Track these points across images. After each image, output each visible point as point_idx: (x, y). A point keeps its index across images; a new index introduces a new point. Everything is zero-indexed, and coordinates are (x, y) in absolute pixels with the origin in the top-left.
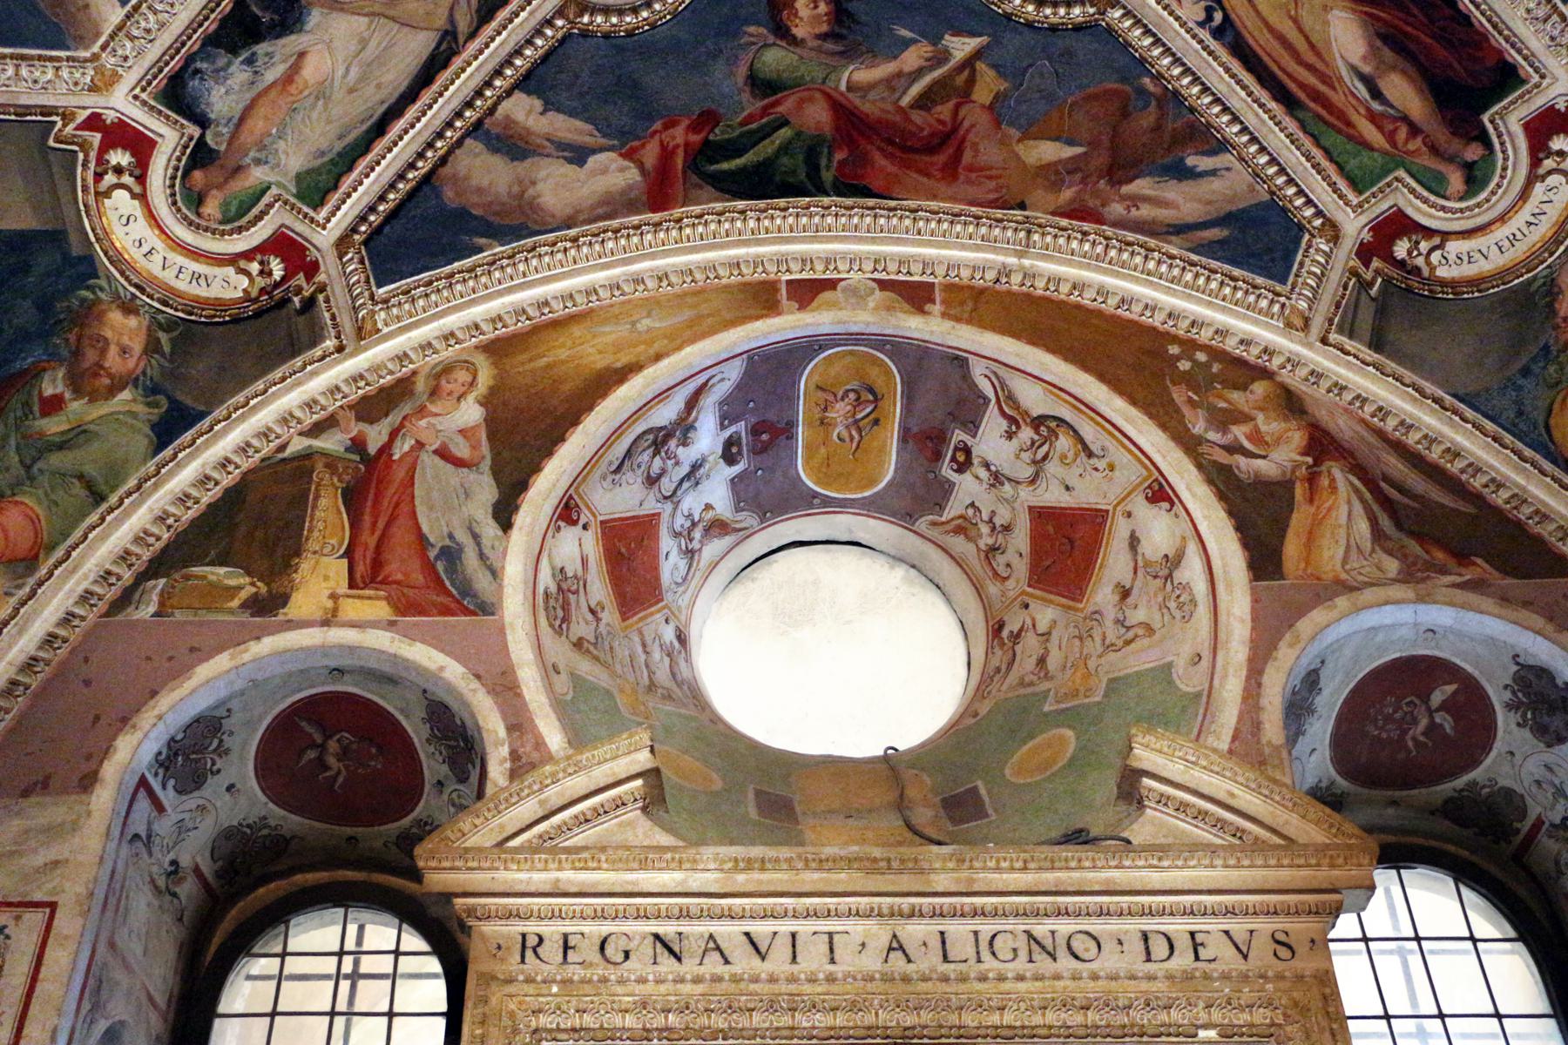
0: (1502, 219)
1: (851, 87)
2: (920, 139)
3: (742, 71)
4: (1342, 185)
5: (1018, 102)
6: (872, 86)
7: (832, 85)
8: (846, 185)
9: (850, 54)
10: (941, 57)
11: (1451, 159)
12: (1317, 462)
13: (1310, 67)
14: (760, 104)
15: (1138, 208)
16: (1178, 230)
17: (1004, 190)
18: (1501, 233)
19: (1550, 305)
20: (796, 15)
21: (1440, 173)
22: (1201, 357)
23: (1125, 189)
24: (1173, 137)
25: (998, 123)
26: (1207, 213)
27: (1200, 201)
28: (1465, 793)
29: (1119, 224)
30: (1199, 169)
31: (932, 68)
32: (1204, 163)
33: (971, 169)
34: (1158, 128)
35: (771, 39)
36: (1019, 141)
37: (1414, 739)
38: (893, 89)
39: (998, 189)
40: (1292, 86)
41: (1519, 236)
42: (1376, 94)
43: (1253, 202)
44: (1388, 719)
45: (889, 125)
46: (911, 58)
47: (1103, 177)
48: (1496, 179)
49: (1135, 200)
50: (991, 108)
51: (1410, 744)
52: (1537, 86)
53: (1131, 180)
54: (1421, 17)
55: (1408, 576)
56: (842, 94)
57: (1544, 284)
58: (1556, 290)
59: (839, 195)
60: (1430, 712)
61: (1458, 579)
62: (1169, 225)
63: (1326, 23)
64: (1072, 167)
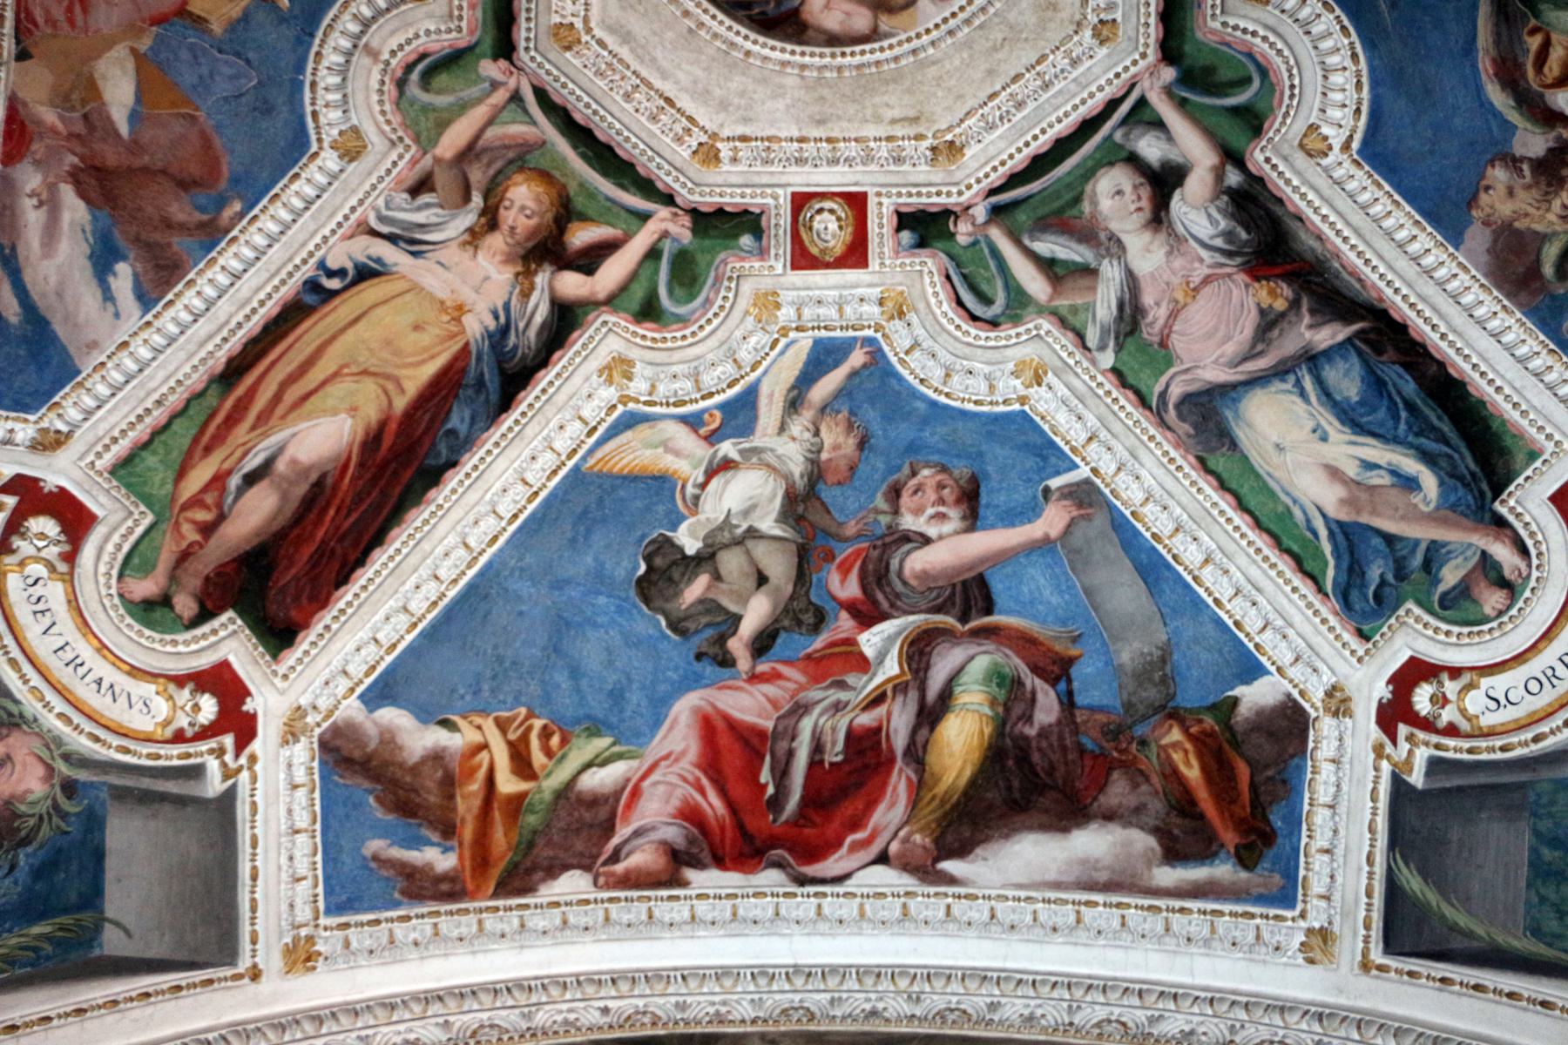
0: (102, 649)
5: (192, 48)
11: (173, 577)
13: (277, 398)
17: (49, 31)
18: (85, 651)
21: (154, 567)
23: (68, 193)
24: (158, 244)
25: (158, 21)
26: (44, 295)
27: (61, 283)
30: (111, 279)
32: (123, 277)
34: (169, 224)
36: (134, 51)
40: (249, 380)
41: (81, 671)
42: (251, 479)
43: (72, 350)
47: (82, 159)
48: (157, 636)
49: (51, 203)
52: (275, 673)
53: (82, 195)
54: (346, 525)
57: (10, 714)
63: (335, 412)
64: (94, 121)
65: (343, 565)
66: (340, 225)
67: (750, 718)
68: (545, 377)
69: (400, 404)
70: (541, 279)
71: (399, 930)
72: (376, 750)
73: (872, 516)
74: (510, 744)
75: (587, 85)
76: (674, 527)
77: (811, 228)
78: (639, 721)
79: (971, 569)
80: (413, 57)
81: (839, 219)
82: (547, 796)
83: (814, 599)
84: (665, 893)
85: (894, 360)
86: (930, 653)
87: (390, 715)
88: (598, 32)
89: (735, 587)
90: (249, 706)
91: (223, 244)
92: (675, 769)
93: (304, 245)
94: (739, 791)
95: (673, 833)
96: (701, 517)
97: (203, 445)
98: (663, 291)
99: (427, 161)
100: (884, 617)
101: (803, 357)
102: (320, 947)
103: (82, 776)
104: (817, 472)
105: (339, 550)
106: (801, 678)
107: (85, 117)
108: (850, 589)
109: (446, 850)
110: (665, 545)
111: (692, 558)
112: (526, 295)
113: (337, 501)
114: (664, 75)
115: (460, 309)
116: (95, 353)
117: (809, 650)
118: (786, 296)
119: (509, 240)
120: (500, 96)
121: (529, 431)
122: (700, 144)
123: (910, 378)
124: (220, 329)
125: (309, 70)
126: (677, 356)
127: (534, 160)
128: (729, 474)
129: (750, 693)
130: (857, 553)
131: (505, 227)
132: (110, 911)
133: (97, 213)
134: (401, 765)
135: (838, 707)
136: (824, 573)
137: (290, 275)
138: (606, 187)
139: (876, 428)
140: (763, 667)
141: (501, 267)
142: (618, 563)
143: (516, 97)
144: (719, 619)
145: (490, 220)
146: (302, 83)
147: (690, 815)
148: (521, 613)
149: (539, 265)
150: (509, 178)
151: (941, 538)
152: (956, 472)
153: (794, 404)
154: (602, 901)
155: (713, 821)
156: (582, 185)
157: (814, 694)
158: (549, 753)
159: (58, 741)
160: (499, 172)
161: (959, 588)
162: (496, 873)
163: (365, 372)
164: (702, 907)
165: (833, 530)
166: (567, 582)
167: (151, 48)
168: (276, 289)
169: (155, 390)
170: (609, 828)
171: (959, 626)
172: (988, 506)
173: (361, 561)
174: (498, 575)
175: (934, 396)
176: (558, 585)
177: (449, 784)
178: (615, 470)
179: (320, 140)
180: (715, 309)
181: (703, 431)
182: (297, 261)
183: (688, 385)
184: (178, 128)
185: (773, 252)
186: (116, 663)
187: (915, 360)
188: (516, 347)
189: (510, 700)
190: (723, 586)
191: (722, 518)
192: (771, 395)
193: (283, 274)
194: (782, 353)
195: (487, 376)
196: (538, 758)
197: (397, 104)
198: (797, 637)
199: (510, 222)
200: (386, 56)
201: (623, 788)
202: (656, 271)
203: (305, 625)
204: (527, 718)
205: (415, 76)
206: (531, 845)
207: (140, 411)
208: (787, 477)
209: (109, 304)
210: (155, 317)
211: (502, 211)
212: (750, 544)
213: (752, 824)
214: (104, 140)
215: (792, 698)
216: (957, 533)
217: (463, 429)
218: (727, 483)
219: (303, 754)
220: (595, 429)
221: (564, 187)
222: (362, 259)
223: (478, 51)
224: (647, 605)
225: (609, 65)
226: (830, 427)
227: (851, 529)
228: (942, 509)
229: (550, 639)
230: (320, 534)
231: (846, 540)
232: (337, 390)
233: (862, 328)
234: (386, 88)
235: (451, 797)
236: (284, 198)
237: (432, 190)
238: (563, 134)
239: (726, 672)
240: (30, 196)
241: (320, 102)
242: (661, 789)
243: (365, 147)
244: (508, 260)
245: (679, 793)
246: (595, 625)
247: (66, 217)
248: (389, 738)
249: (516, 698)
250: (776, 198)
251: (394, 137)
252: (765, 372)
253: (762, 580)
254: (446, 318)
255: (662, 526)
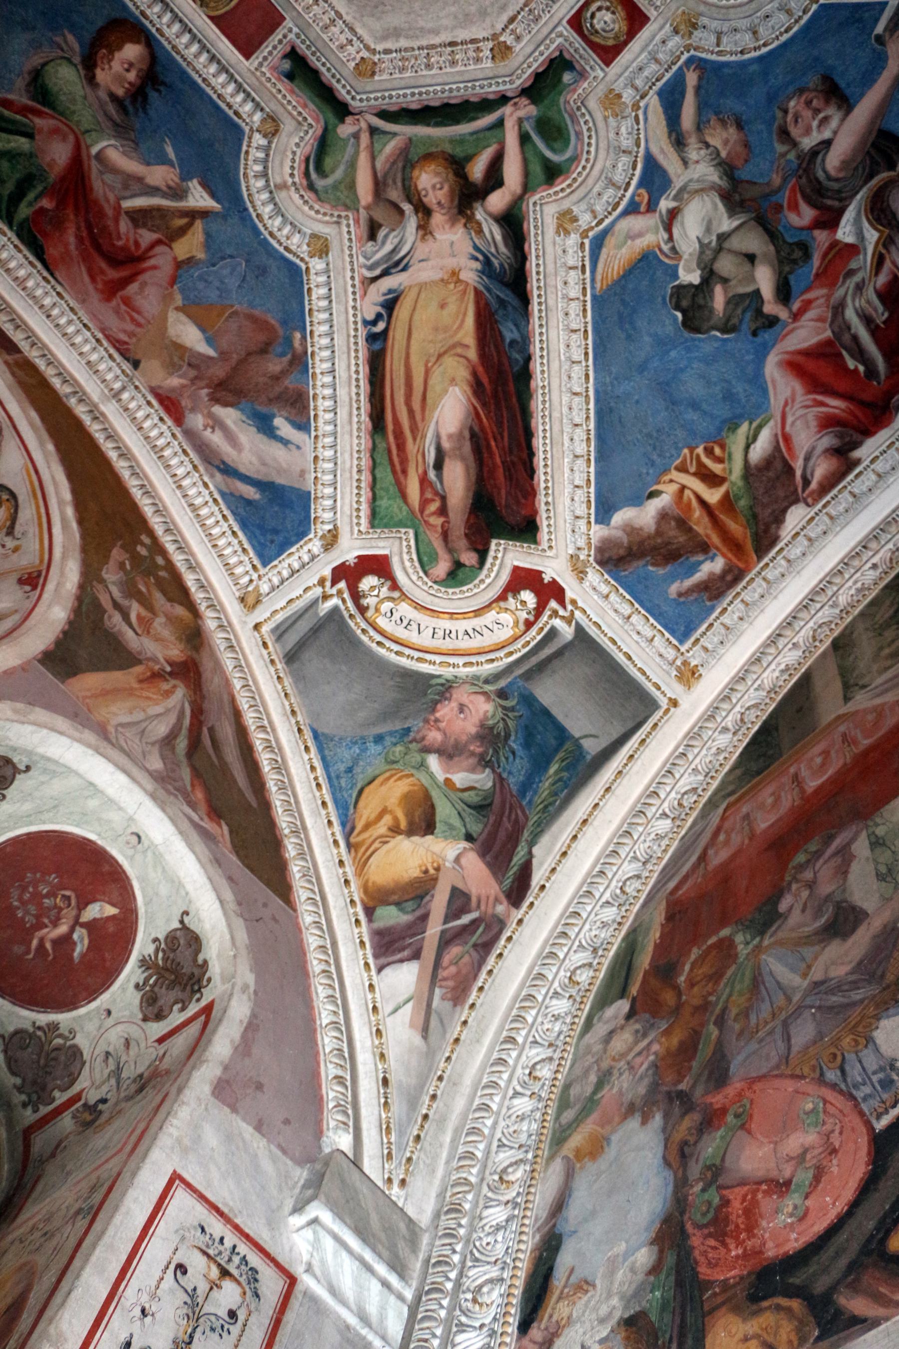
1: (99, 157)
2: (114, 245)
3: (36, 60)
4: (365, 508)
5: (201, 278)
6: (115, 170)
7: (89, 141)
8: (30, 231)
9: (121, 130)
10: (178, 193)
11: (450, 550)
12: (171, 674)
13: (411, 412)
14: (25, 101)
15: (213, 431)
16: (228, 470)
17: (134, 340)
18: (446, 624)
19: (436, 703)
20: (110, 61)
21: (437, 554)
22: (160, 561)
24: (281, 393)
25: (173, 281)
26: (258, 472)
28: (39, 1033)
29: (190, 435)
30: (279, 433)
31: (165, 195)
33: (127, 301)
34: (276, 378)
35: (77, 59)
36: (177, 309)
37: (42, 941)
38: (126, 187)
39: (131, 335)
41: (453, 635)
42: (439, 466)
43: (297, 486)
44: (37, 897)
45: (101, 214)
46: (158, 175)
47: (208, 386)
48: (471, 586)
49: (217, 424)
50: (179, 265)
51: (35, 943)
52: (544, 550)
53: (226, 405)
55: (160, 779)
56: (89, 155)
57: (442, 685)
58: (448, 695)
59: (19, 235)
60: (76, 922)
61: (196, 818)
62: (223, 462)
63: (446, 391)
64: (196, 362)
65: (524, 464)
66: (354, 293)
67: (814, 340)
68: (532, 265)
69: (472, 354)
70: (479, 215)
71: (725, 619)
72: (630, 542)
73: (782, 161)
74: (695, 474)
75: (403, 83)
76: (676, 277)
77: (597, 32)
78: (753, 399)
79: (870, 133)
80: (303, 166)
81: (608, 9)
82: (740, 483)
83: (790, 240)
84: (851, 477)
85: (714, 57)
86: (889, 206)
87: (620, 517)
88: (379, 47)
89: (740, 277)
90: (547, 579)
91: (310, 362)
92: (797, 405)
93: (347, 322)
94: (843, 385)
95: (827, 441)
96: (685, 257)
97: (400, 472)
98: (548, 154)
99: (363, 213)
100: (841, 212)
101: (660, 110)
102: (694, 663)
103: (502, 683)
104: (727, 168)
105: (515, 459)
106: (824, 291)
107: (189, 365)
108: (808, 214)
109: (712, 559)
110: (680, 291)
111: (701, 284)
112: (480, 231)
113: (490, 435)
114: (436, 32)
115: (454, 274)
116: (307, 476)
117: (814, 271)
118: (618, 86)
119: (443, 211)
120: (365, 138)
121: (551, 302)
122: (491, 50)
123: (733, 58)
124: (351, 406)
125: (262, 229)
126: (590, 181)
127: (414, 156)
128: (679, 218)
129: (802, 327)
130: (793, 190)
131: (435, 207)
132: (577, 734)
133: (241, 406)
134: (649, 537)
135: (859, 287)
136: (784, 221)
137: (356, 343)
138: (464, 128)
139: (739, 108)
140: (796, 306)
141: (454, 230)
142: (664, 326)
143: (373, 131)
144: (747, 302)
145: (424, 211)
146: (265, 239)
147: (827, 423)
148: (637, 402)
149: (471, 208)
150: (411, 178)
151: (835, 133)
152: (811, 85)
153: (679, 142)
154: (820, 511)
155: (843, 415)
156: (452, 141)
157: (840, 292)
158: (720, 460)
159: (476, 677)
160: (403, 180)
161: (873, 152)
162: (749, 546)
163: (440, 356)
164: (879, 466)
165: (767, 191)
166: (646, 361)
167: (183, 299)
168: (357, 357)
169: (351, 467)
170: (790, 470)
171: (892, 173)
172: (848, 85)
173: (531, 454)
174: (606, 392)
175: (758, 53)
176: (642, 368)
177: (683, 524)
178: (615, 277)
179: (302, 260)
180: (586, 134)
181: (643, 208)
182: (352, 333)
183: (611, 191)
184: (233, 325)
185: (588, 68)
186: (464, 615)
187: (727, 44)
188: (501, 265)
189: (673, 452)
190: (733, 283)
191: (697, 246)
192: (662, 151)
193: (353, 347)
194: (646, 120)
195: (502, 295)
196: (717, 468)
197: (320, 199)
198: (800, 271)
199: (434, 201)
200: (290, 181)
201: (778, 442)
202: (534, 145)
203: (535, 512)
204: (691, 453)
205: (314, 176)
206: (755, 516)
207: (355, 484)
208: (713, 187)
209: (290, 446)
210: (316, 430)
211: (425, 200)
212: (726, 245)
213: (866, 396)
214: (208, 367)
215: (828, 307)
216: (843, 120)
217: (516, 335)
218: (682, 224)
219: (594, 576)
220: (583, 266)
221: (443, 152)
222: (382, 299)
223: (330, 127)
224: (700, 333)
225: (403, 59)
226: (712, 135)
227: (777, 180)
228: (821, 115)
229: (665, 400)
230: (498, 460)
231: (779, 189)
232: (435, 379)
233: (679, 58)
234: (306, 198)
235: (690, 529)
236: (315, 308)
237: (380, 226)
238: (416, 124)
239: (777, 328)
240: (205, 429)
241: (283, 240)
242: (798, 423)
243: (327, 239)
244: (453, 222)
245: (810, 417)
246: (682, 370)
247: (229, 422)
248: (630, 529)
249: (677, 448)
250: (560, 35)
251: (335, 219)
252: (647, 141)
253: (751, 258)
254: (452, 286)
255: (670, 283)
